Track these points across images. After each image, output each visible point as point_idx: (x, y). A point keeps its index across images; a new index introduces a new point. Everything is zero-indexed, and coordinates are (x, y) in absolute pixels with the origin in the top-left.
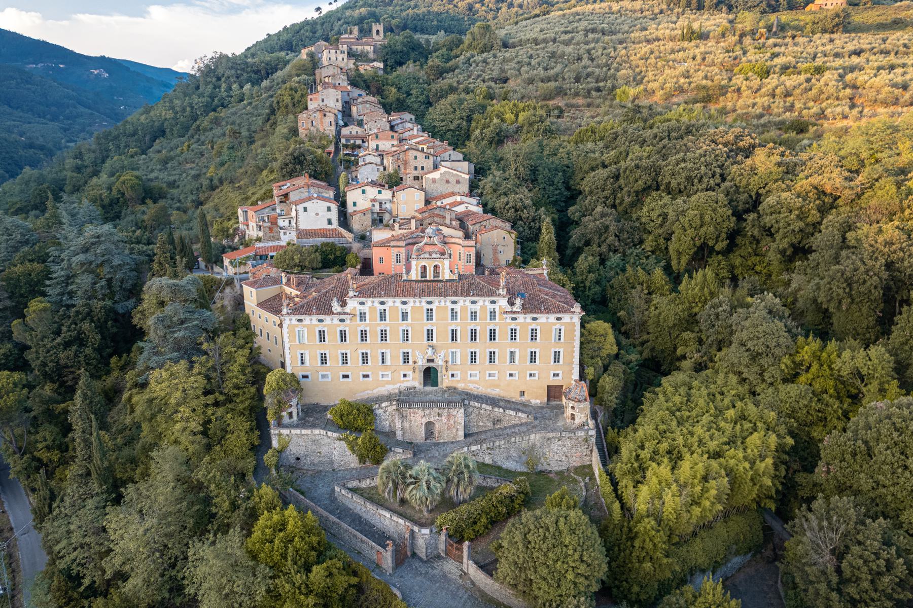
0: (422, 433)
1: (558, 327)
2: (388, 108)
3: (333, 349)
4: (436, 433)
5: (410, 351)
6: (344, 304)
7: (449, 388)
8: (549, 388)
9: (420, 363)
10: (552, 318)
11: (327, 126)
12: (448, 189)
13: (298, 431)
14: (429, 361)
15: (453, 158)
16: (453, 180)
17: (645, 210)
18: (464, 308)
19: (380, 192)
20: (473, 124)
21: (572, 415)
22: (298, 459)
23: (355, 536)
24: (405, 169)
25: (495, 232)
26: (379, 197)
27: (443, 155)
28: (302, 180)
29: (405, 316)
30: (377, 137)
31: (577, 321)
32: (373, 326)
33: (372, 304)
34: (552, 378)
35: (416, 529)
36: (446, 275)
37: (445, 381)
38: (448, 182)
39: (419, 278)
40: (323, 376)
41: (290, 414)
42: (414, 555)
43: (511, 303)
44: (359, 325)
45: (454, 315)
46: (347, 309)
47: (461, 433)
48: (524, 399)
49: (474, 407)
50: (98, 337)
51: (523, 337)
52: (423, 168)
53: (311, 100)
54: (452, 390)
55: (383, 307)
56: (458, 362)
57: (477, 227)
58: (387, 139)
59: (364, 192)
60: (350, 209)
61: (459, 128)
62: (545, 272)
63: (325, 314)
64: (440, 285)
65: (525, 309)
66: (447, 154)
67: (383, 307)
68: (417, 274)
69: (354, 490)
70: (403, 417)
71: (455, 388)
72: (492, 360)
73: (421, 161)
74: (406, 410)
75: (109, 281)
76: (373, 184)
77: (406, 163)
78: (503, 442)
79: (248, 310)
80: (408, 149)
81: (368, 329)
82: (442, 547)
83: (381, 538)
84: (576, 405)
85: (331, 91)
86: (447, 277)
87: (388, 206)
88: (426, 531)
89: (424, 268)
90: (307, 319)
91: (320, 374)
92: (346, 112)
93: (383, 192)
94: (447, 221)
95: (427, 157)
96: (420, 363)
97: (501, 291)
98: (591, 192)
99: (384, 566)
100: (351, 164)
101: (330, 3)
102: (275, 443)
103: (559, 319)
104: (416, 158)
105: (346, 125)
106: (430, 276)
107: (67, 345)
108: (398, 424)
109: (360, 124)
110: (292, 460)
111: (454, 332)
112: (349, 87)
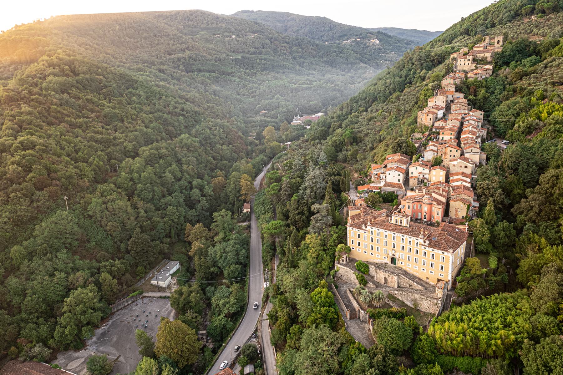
1: (443, 256)
3: (363, 243)
6: (366, 227)
14: (393, 255)
15: (473, 151)
26: (423, 172)
33: (375, 229)
37: (399, 264)
38: (461, 167)
41: (343, 261)
42: (359, 318)
46: (367, 229)
48: (427, 281)
52: (454, 156)
54: (400, 269)
58: (448, 135)
59: (416, 168)
60: (410, 175)
66: (470, 149)
75: (316, 192)
77: (445, 153)
87: (427, 176)
90: (354, 229)
102: (336, 268)
106: (399, 223)
107: (299, 214)
110: (340, 276)
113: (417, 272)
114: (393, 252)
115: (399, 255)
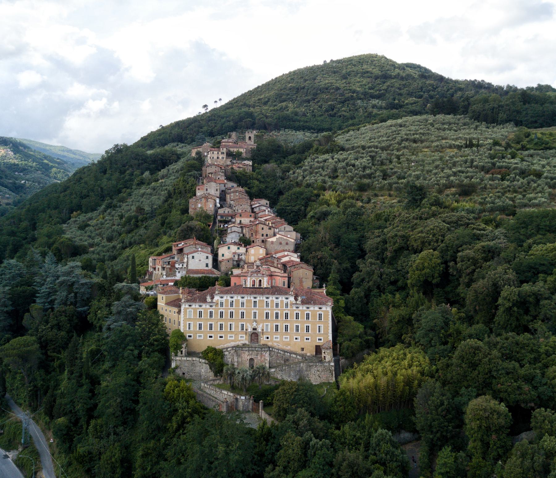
2: (252, 196)
5: (244, 323)
6: (212, 298)
8: (316, 346)
11: (210, 207)
12: (281, 248)
13: (185, 359)
15: (287, 229)
16: (284, 243)
17: (400, 262)
18: (272, 301)
19: (238, 248)
20: (309, 208)
22: (184, 374)
23: (210, 399)
24: (256, 235)
25: (301, 270)
26: (238, 251)
27: (280, 228)
28: (191, 242)
30: (241, 216)
31: (329, 310)
34: (318, 341)
35: (238, 397)
36: (265, 284)
37: (263, 340)
38: (281, 243)
40: (200, 336)
41: (182, 351)
43: (296, 299)
44: (220, 309)
45: (267, 305)
46: (214, 300)
50: (69, 325)
52: (267, 235)
53: (199, 189)
55: (232, 300)
56: (269, 331)
57: (293, 268)
58: (247, 217)
59: (229, 248)
60: (220, 258)
61: (300, 210)
62: (325, 291)
63: (203, 302)
64: (261, 290)
65: (303, 303)
66: (283, 227)
67: (232, 300)
70: (238, 356)
73: (266, 231)
74: (240, 352)
76: (235, 243)
77: (256, 232)
78: (287, 367)
79: (159, 308)
80: (258, 224)
82: (251, 407)
84: (326, 351)
85: (213, 184)
86: (265, 286)
87: (243, 257)
88: (243, 398)
91: (198, 335)
92: (223, 197)
93: (241, 248)
94: (275, 265)
95: (270, 229)
96: (249, 330)
100: (223, 233)
101: (216, 102)
102: (173, 365)
103: (320, 308)
104: (263, 229)
105: (222, 207)
106: (257, 285)
107: (52, 328)
108: (236, 359)
109: (230, 206)
111: (267, 314)
112: (225, 181)
114: (255, 324)
115: (263, 326)
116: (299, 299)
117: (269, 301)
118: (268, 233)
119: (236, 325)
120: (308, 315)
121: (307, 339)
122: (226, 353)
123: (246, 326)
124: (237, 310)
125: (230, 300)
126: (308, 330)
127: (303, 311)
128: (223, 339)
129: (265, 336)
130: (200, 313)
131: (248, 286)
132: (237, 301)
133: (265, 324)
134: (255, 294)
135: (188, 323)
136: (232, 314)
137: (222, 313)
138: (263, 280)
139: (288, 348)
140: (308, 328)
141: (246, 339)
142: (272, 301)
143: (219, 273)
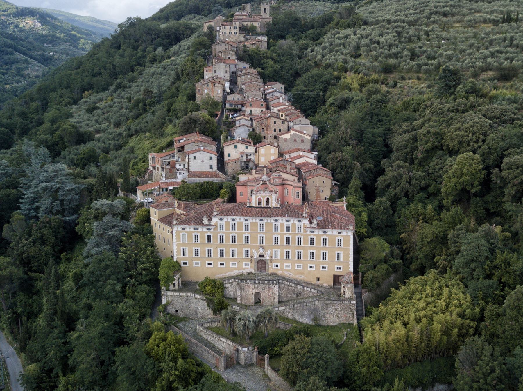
0: (253, 300)
2: (265, 78)
4: (262, 301)
5: (249, 249)
6: (210, 220)
7: (272, 274)
9: (255, 257)
10: (335, 232)
11: (217, 93)
12: (295, 146)
14: (261, 256)
15: (302, 123)
18: (282, 224)
19: (247, 148)
20: (328, 94)
21: (344, 292)
22: (177, 311)
23: (205, 350)
24: (267, 130)
25: (318, 178)
26: (246, 151)
27: (295, 121)
28: (195, 136)
29: (247, 227)
30: (251, 105)
31: (350, 234)
32: (228, 233)
33: (228, 220)
35: (240, 348)
36: (273, 203)
38: (295, 141)
39: (257, 206)
40: (196, 264)
41: (174, 284)
42: (238, 363)
43: (311, 222)
44: (219, 233)
45: (276, 228)
46: (212, 223)
47: (276, 300)
48: (319, 282)
49: (285, 284)
51: (317, 244)
52: (280, 130)
53: (207, 71)
54: (274, 274)
55: (234, 222)
56: (279, 258)
57: (308, 173)
58: (258, 107)
59: (236, 147)
60: (226, 158)
61: (318, 95)
62: (345, 205)
63: (199, 225)
64: (269, 210)
65: (320, 226)
66: (298, 120)
67: (234, 222)
68: (256, 203)
69: (207, 328)
70: (242, 289)
71: (276, 274)
72: (299, 257)
73: (279, 125)
74: (243, 284)
76: (243, 141)
77: (268, 126)
78: (299, 305)
79: (152, 223)
80: (270, 117)
81: (224, 235)
82: (254, 360)
83: (219, 352)
84: (346, 285)
85: (222, 65)
86: (274, 205)
87: (252, 157)
88: (245, 349)
89: (260, 200)
91: (194, 262)
92: (233, 81)
93: (249, 147)
94: (288, 170)
95: (283, 123)
96: (255, 257)
97: (304, 215)
98: (397, 150)
99: (220, 367)
100: (231, 125)
103: (340, 233)
104: (275, 123)
105: (232, 92)
108: (239, 293)
109: (241, 92)
111: (276, 239)
112: (236, 61)
113: (302, 274)
114: (261, 250)
115: (271, 253)
116: (315, 222)
117: (278, 224)
118: (281, 128)
119: (239, 250)
120: (325, 240)
121: (323, 267)
122: (228, 285)
123: (252, 252)
124: (241, 234)
125: (232, 222)
126: (324, 257)
127: (318, 236)
128: (224, 266)
129: (274, 264)
130: (196, 237)
131: (254, 205)
132: (240, 223)
133: (274, 250)
134: (262, 216)
135: (182, 248)
136: (234, 239)
137: (222, 238)
138: (272, 198)
139: (301, 277)
140: (324, 255)
141: (251, 267)
142: (282, 224)
143: (225, 176)
